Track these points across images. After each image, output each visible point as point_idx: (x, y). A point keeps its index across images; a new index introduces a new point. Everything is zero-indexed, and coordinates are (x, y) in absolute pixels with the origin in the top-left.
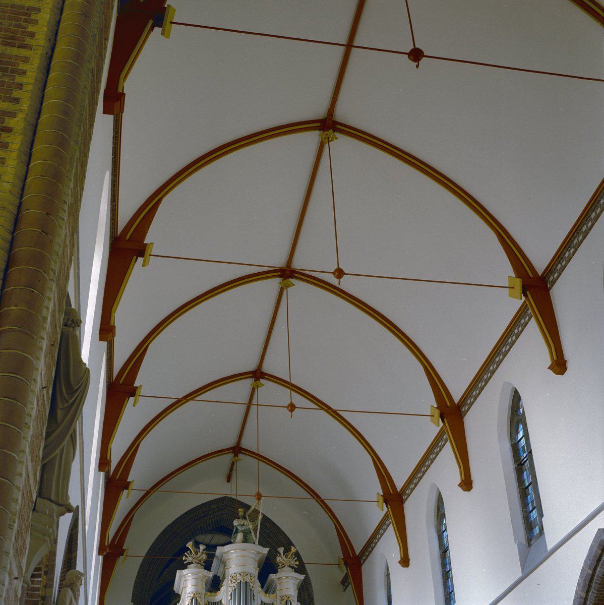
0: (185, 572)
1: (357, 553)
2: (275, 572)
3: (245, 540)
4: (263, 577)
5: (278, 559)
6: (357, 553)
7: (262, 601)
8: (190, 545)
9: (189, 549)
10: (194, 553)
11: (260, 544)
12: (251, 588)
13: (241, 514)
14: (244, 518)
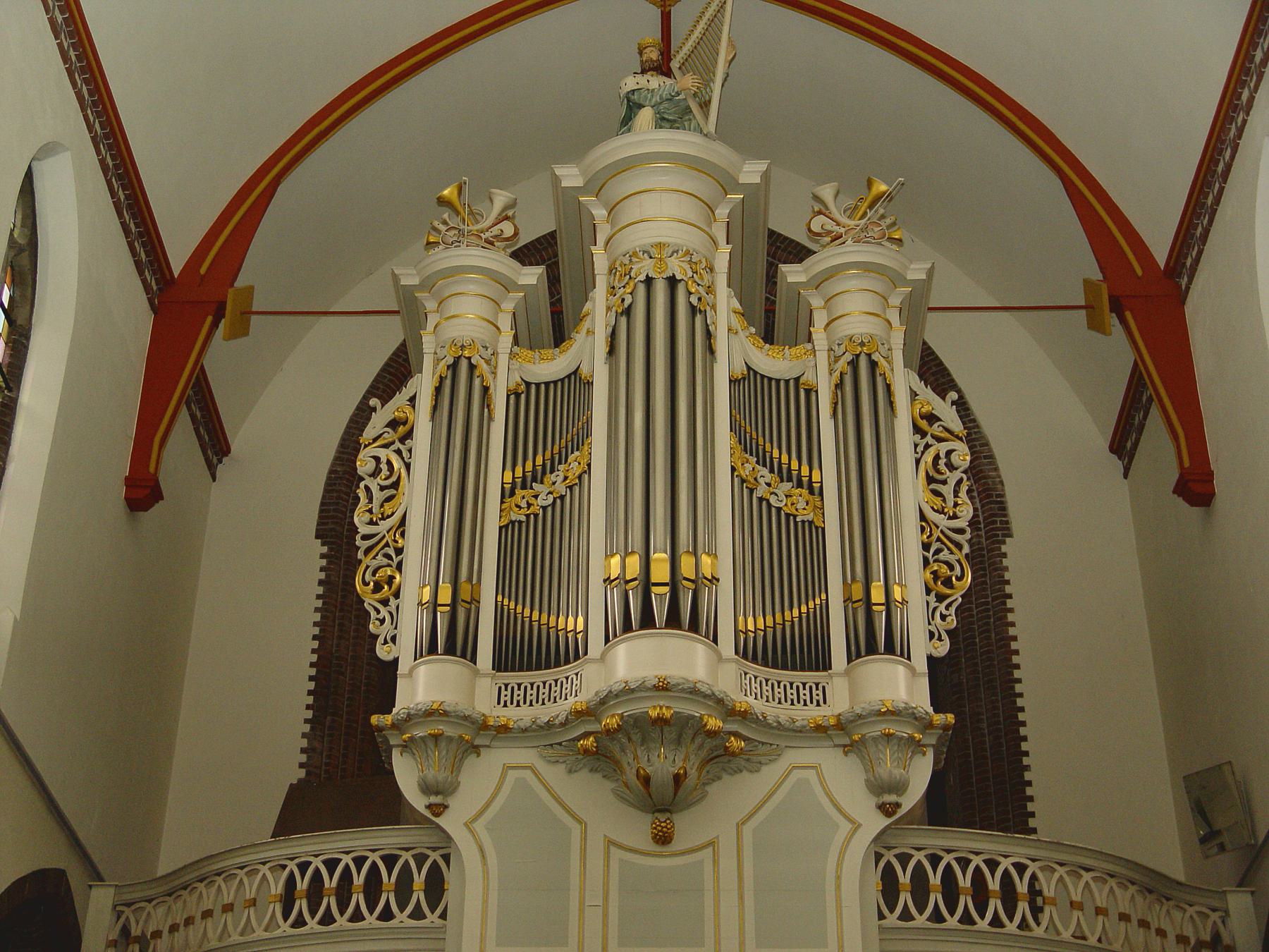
7: (749, 368)
12: (694, 300)
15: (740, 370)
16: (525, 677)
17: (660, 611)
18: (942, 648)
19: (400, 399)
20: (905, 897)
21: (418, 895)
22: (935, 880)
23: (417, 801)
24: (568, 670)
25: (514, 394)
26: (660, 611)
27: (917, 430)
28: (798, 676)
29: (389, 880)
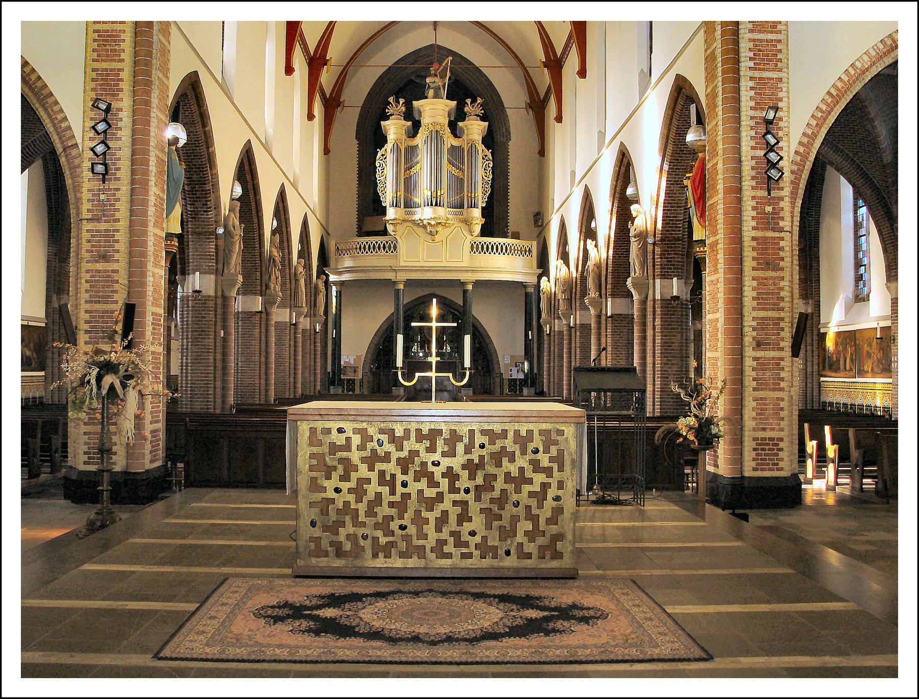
0: (387, 122)
1: (542, 97)
2: (463, 120)
3: (437, 96)
4: (453, 126)
5: (466, 109)
6: (542, 97)
8: (391, 99)
9: (391, 103)
10: (396, 107)
11: (447, 98)
13: (432, 72)
14: (436, 76)
15: (449, 146)
16: (410, 209)
17: (434, 204)
18: (484, 205)
19: (383, 149)
20: (475, 249)
21: (392, 249)
22: (480, 246)
23: (392, 233)
24: (417, 209)
25: (406, 149)
26: (434, 203)
27: (483, 158)
28: (458, 210)
29: (387, 246)
